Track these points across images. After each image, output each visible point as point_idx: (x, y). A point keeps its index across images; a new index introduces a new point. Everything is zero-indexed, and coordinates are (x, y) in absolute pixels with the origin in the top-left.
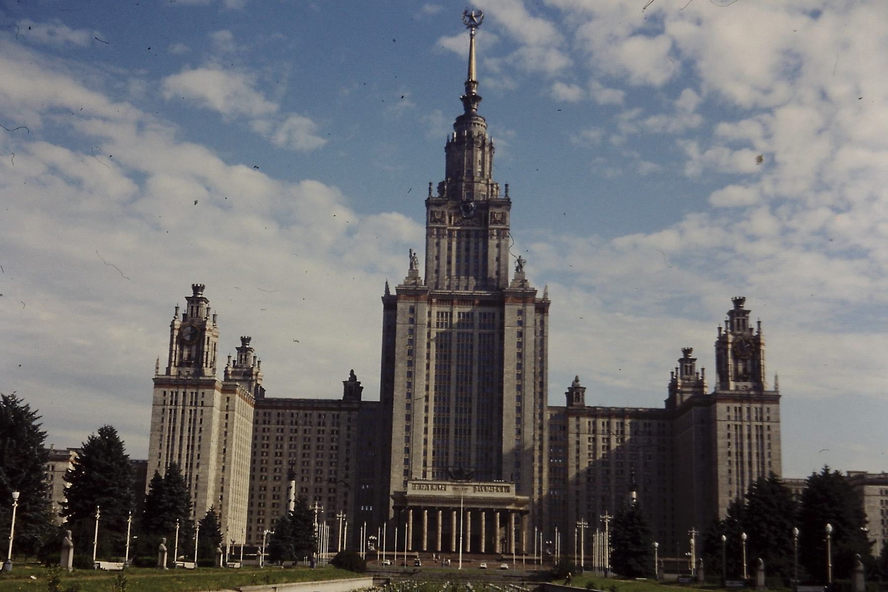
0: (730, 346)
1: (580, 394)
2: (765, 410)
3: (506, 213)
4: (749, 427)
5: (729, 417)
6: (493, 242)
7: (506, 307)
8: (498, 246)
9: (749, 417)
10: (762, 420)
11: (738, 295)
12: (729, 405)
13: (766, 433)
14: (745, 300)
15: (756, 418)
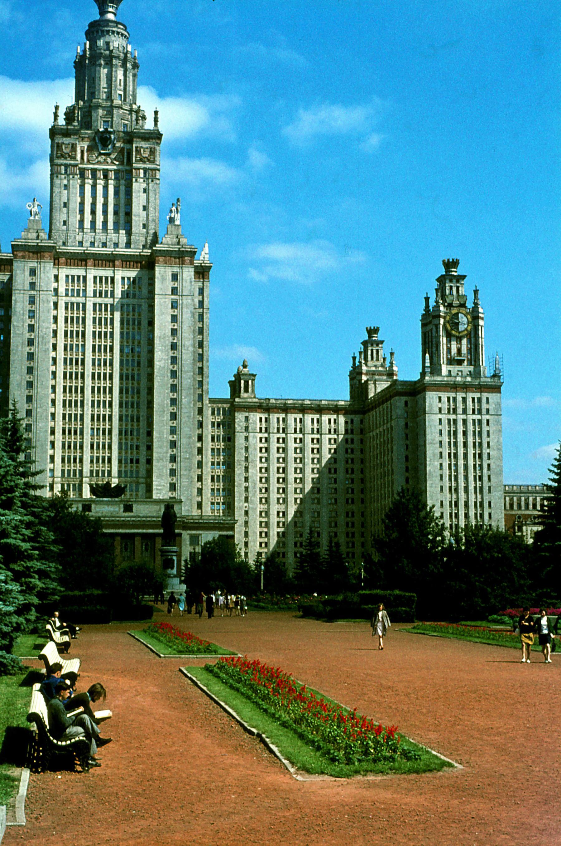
0: (442, 321)
1: (250, 382)
2: (484, 401)
3: (154, 148)
4: (465, 422)
5: (440, 409)
6: (138, 186)
7: (157, 269)
8: (145, 191)
9: (465, 411)
10: (480, 412)
11: (451, 256)
12: (441, 394)
13: (485, 428)
14: (459, 263)
15: (474, 410)
